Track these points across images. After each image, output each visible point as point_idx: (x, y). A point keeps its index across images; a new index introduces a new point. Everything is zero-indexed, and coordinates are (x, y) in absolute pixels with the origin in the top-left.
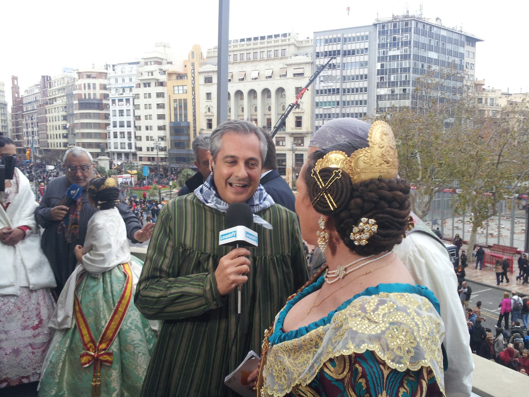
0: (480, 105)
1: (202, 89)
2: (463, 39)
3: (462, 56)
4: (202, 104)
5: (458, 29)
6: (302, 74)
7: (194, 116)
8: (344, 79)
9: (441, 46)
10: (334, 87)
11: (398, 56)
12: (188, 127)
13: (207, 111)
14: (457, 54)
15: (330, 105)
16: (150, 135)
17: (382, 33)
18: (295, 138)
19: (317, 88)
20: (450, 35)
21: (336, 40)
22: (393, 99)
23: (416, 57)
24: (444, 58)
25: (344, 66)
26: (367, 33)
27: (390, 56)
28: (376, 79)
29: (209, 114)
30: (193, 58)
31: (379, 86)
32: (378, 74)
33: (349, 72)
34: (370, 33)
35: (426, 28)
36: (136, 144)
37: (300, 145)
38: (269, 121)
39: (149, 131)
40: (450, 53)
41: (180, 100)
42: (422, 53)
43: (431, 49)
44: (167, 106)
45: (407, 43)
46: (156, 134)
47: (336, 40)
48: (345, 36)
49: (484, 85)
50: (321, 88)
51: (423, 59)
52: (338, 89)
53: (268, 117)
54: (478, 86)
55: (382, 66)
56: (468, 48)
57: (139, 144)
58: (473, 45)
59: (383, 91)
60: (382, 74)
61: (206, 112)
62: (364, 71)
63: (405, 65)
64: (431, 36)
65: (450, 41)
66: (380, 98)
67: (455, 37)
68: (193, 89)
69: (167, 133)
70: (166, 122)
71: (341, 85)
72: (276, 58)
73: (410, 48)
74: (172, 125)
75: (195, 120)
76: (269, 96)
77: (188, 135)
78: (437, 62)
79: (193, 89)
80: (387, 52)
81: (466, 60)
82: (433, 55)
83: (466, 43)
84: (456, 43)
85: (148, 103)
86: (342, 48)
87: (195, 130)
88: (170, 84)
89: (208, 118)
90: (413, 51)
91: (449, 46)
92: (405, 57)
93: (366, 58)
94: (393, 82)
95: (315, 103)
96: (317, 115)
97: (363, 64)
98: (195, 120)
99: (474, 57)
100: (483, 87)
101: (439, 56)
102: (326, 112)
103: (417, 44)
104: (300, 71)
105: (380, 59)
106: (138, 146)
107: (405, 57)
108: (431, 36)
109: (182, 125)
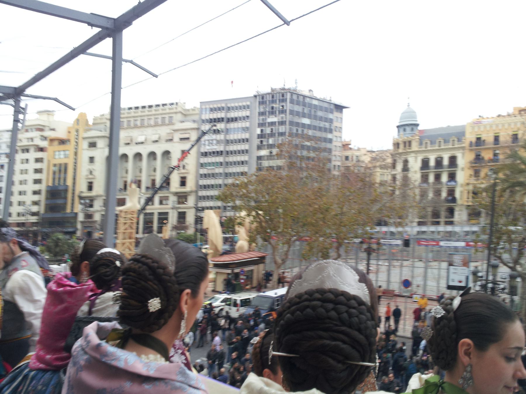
0: (347, 162)
1: (85, 153)
2: (332, 107)
3: (331, 121)
4: (84, 167)
5: (328, 99)
6: (188, 139)
7: (74, 179)
8: (228, 142)
9: (313, 113)
10: (218, 150)
11: (275, 122)
12: (66, 191)
14: (326, 120)
15: (213, 166)
17: (262, 103)
19: (203, 150)
20: (322, 104)
21: (220, 109)
22: (271, 159)
23: (291, 123)
24: (317, 123)
25: (227, 131)
26: (248, 103)
27: (269, 123)
28: (256, 142)
29: (91, 176)
30: (78, 124)
31: (259, 148)
32: (258, 138)
33: (231, 137)
34: (251, 103)
35: (298, 98)
37: (183, 203)
38: (153, 181)
40: (321, 119)
42: (296, 119)
43: (304, 116)
44: (45, 171)
45: (283, 111)
46: (30, 198)
47: (220, 109)
48: (229, 105)
49: (350, 144)
50: (206, 151)
51: (298, 124)
52: (222, 152)
53: (153, 178)
54: (346, 146)
55: (262, 131)
56: (336, 114)
58: (341, 112)
59: (264, 153)
60: (262, 138)
61: (87, 176)
62: (246, 135)
63: (282, 130)
64: (304, 105)
65: (321, 108)
66: (259, 158)
67: (326, 105)
68: (76, 154)
71: (225, 148)
72: (163, 124)
73: (286, 115)
74: (49, 189)
75: (74, 183)
76: (155, 159)
77: (65, 198)
78: (309, 127)
79: (76, 154)
80: (266, 119)
81: (335, 124)
82: (306, 121)
83: (334, 110)
84: (326, 110)
86: (226, 116)
87: (73, 194)
88: (51, 149)
89: (89, 181)
90: (288, 118)
91: (320, 113)
92: (282, 123)
93: (247, 124)
94: (271, 145)
95: (200, 165)
96: (201, 175)
97: (245, 129)
99: (341, 122)
100: (350, 146)
101: (311, 122)
102: (210, 172)
103: (292, 112)
104: (186, 136)
105: (260, 125)
107: (282, 123)
108: (304, 105)
109: (61, 188)
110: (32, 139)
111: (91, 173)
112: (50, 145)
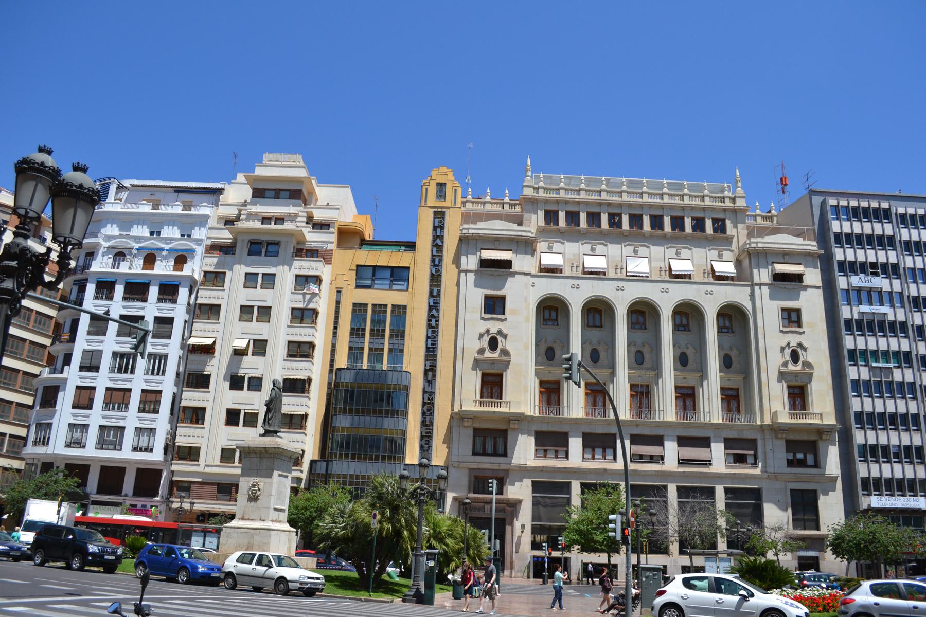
7: (431, 352)
10: (891, 318)
13: (486, 345)
18: (791, 445)
36: (173, 435)
41: (380, 309)
57: (187, 436)
61: (481, 351)
68: (435, 279)
69: (312, 406)
70: (316, 371)
79: (435, 279)
85: (256, 304)
98: (430, 372)
106: (181, 441)
110: (280, 220)
112: (340, 245)
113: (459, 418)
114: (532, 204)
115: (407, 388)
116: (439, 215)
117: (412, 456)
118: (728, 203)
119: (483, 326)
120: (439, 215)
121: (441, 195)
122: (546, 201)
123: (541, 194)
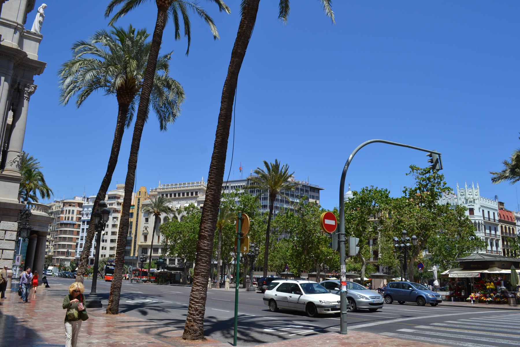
16: (104, 246)
39: (104, 243)
61: (144, 231)
98: (136, 236)
110: (112, 204)
111: (146, 229)
113: (140, 246)
114: (159, 193)
115: (131, 240)
116: (139, 199)
117: (132, 255)
118: (199, 187)
119: (144, 225)
120: (139, 199)
121: (140, 195)
122: (162, 192)
123: (161, 190)
